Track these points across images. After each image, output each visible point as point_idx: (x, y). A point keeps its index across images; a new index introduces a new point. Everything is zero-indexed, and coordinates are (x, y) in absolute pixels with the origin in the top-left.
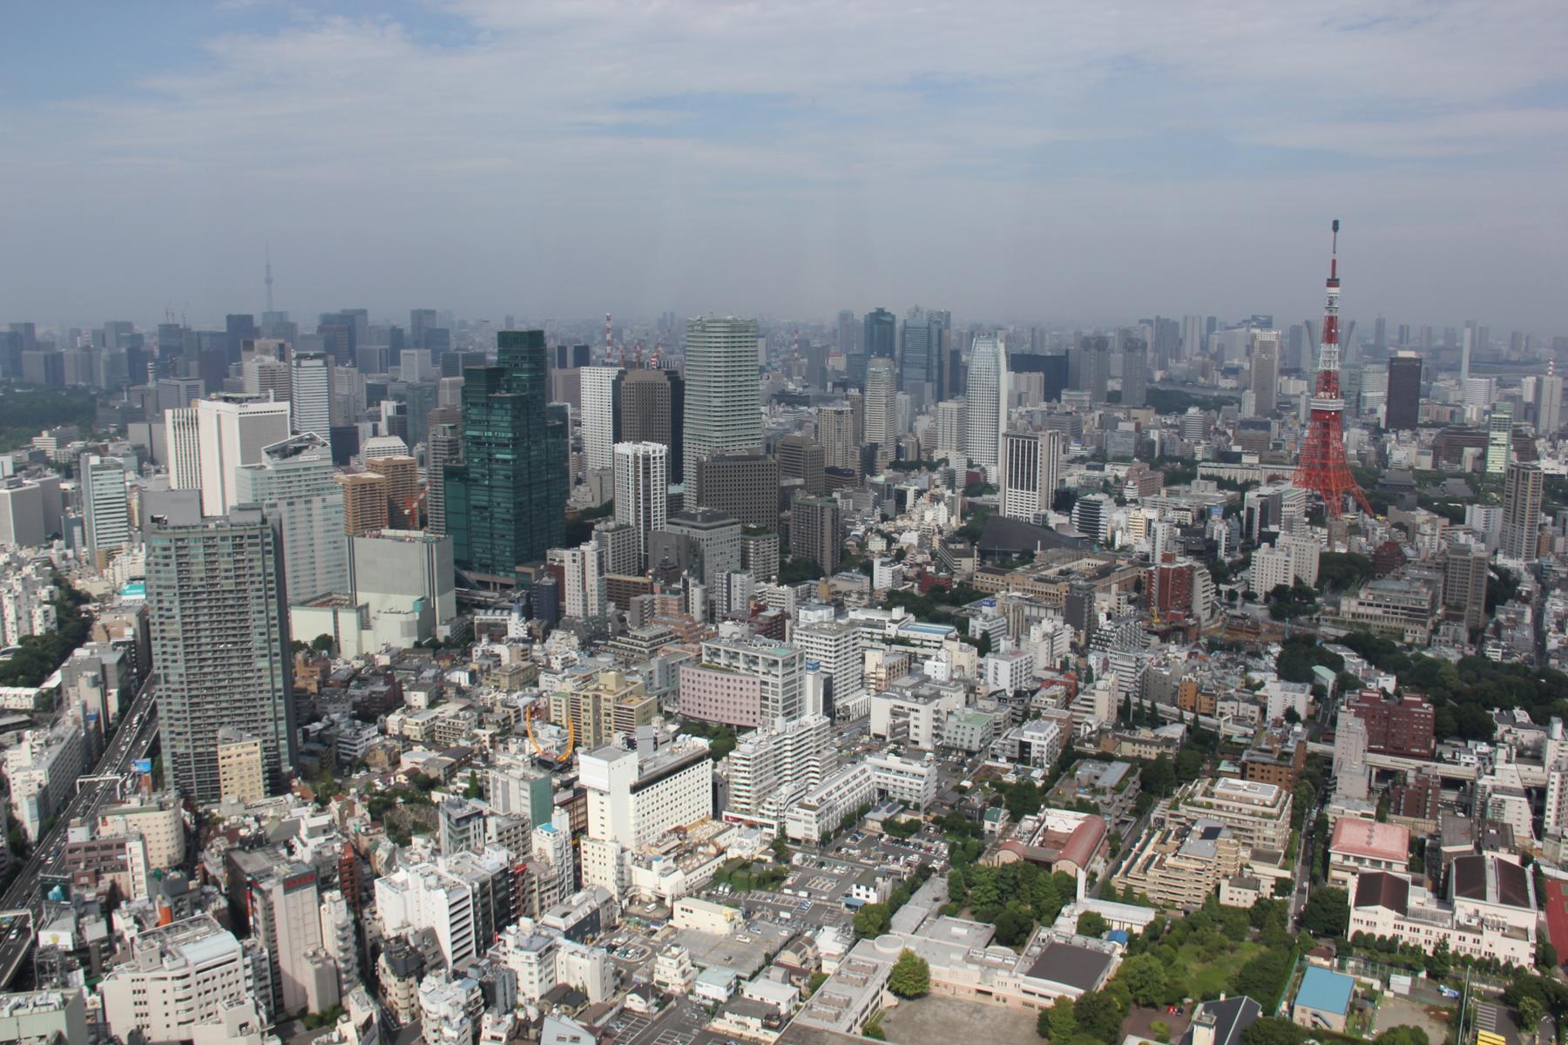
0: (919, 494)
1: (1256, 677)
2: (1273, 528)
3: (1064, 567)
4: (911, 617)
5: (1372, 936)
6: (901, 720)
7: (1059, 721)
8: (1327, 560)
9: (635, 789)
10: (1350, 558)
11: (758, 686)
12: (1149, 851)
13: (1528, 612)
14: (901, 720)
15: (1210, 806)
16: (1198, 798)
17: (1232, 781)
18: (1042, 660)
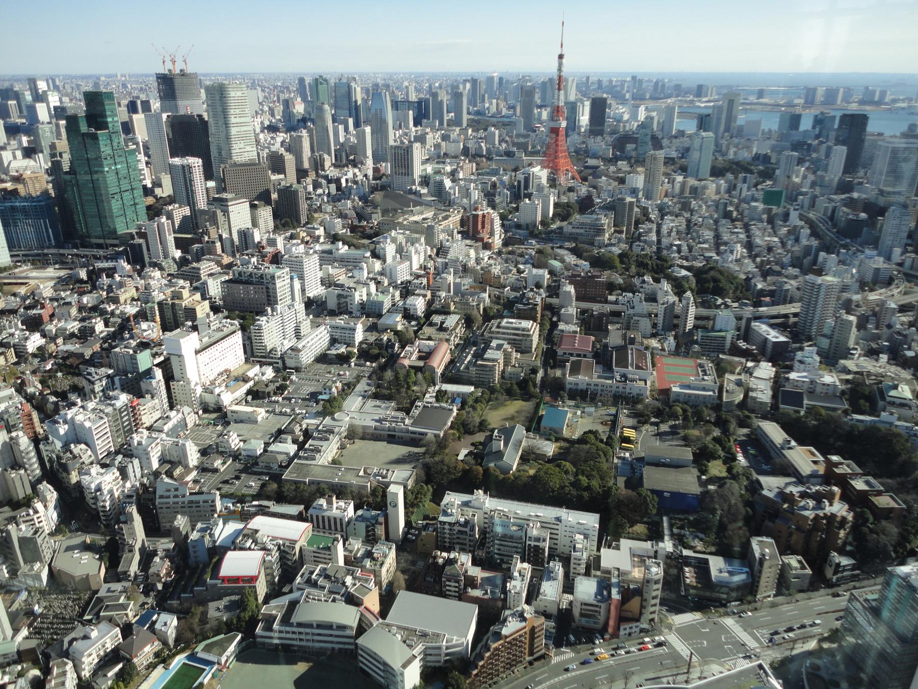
0: (347, 180)
1: (521, 267)
2: (530, 191)
3: (424, 216)
4: (346, 247)
5: (577, 390)
6: (343, 300)
7: (425, 296)
8: (556, 205)
9: (197, 352)
10: (569, 205)
11: (265, 290)
12: (469, 357)
13: (654, 227)
14: (343, 300)
15: (498, 333)
16: (494, 329)
17: (510, 320)
18: (415, 266)
